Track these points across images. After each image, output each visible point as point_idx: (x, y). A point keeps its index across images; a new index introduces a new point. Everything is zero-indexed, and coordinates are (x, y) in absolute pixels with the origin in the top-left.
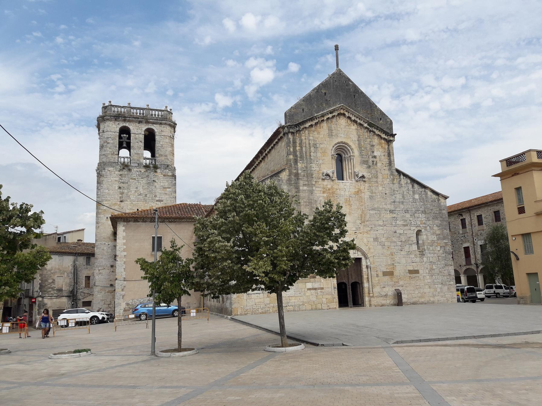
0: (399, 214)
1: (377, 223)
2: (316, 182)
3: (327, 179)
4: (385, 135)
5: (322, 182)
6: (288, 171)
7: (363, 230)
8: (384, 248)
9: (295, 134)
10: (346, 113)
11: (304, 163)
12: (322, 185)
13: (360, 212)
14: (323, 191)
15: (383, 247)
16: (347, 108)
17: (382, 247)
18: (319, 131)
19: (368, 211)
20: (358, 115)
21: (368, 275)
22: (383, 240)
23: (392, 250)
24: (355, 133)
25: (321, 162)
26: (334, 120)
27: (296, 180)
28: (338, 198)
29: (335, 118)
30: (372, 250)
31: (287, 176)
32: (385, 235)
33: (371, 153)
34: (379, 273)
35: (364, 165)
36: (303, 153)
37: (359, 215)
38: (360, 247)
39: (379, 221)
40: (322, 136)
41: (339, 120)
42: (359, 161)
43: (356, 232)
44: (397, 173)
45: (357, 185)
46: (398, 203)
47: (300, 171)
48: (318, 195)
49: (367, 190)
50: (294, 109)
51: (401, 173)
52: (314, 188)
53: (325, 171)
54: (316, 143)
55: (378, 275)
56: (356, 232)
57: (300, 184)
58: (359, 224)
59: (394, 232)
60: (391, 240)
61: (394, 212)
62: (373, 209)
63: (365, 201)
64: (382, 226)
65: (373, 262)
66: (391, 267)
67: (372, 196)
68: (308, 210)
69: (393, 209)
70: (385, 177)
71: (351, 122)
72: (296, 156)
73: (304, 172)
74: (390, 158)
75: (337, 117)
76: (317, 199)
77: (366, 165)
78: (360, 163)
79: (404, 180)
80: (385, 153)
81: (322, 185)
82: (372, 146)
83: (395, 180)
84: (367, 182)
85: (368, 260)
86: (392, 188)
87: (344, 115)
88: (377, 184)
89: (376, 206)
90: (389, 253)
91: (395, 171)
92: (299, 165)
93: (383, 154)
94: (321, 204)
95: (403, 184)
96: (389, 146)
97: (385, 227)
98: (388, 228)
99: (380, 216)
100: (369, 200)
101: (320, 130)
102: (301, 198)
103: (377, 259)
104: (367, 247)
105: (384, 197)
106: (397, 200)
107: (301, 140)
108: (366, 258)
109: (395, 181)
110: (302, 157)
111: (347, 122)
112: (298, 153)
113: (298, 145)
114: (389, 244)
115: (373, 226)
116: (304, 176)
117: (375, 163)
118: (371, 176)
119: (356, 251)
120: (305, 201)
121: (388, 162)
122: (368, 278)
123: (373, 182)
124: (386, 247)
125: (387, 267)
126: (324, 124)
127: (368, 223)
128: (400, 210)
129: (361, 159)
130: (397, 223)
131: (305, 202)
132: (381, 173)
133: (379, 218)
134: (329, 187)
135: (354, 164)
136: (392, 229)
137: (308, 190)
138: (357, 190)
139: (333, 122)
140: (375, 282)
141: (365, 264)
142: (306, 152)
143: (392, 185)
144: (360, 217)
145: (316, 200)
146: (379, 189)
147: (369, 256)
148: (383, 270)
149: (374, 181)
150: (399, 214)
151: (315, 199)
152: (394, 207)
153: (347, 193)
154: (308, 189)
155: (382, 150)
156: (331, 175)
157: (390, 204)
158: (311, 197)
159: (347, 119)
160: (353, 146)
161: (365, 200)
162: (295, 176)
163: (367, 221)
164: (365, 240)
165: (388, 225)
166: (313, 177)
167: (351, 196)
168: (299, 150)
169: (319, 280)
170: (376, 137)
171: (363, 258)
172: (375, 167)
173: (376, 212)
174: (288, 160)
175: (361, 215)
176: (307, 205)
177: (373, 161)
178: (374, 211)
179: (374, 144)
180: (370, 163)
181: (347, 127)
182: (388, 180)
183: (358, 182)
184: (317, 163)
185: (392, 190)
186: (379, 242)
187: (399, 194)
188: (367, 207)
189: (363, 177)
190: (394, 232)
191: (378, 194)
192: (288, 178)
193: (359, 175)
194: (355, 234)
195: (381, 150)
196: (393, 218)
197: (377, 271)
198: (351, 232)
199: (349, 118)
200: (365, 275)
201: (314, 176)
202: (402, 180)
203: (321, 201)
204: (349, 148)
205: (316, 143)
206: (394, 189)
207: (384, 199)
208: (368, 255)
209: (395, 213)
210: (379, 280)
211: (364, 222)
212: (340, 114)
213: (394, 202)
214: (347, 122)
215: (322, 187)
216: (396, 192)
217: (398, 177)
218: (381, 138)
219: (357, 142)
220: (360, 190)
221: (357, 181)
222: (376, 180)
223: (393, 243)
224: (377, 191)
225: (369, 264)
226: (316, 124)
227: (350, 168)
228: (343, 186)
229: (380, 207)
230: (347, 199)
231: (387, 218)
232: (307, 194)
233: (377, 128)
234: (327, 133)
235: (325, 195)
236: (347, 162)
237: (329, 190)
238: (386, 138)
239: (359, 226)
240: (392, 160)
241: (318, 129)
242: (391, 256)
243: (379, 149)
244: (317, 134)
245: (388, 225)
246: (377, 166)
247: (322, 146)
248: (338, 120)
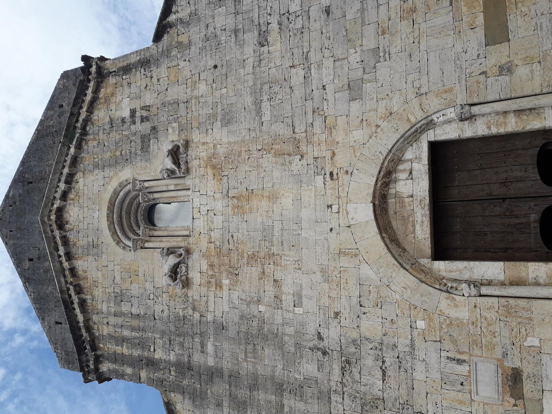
0: (269, 8)
1: (299, 93)
2: (194, 309)
3: (187, 271)
4: (87, 88)
5: (195, 287)
6: (172, 395)
7: (323, 147)
8: (385, 53)
9: (99, 353)
10: (55, 206)
11: (155, 339)
12: (202, 288)
13: (268, 160)
14: (216, 288)
15: (382, 54)
16: (46, 205)
17: (382, 59)
18: (92, 282)
19: (264, 128)
20: (54, 174)
21: (505, 113)
22: (354, 58)
23: (393, 16)
24: (90, 178)
25: (148, 285)
26: (71, 236)
27: (192, 373)
28: (232, 236)
29: (68, 234)
30: (396, 104)
31: (184, 398)
32: (339, 53)
33: (126, 126)
34: (493, 61)
35: (151, 148)
36: (135, 338)
37: (276, 163)
38: (382, 158)
39: (293, 84)
40: (100, 274)
41: (71, 225)
42: (143, 164)
43: (331, 174)
44: (165, 37)
45: (198, 170)
46: (240, 17)
47: (172, 357)
48: (226, 309)
49: (210, 136)
50: (57, 349)
51: (164, 22)
52: (210, 318)
53: (163, 280)
54: (113, 294)
55: (501, 68)
56: (331, 174)
57: (202, 362)
58: (304, 162)
59: (328, 14)
60: (355, 23)
61: (264, 28)
62: (259, 112)
63: (238, 141)
64: (309, 68)
65: (444, 96)
66: (464, 9)
67: (223, 119)
68: (266, 350)
69: (256, 33)
70: (175, 76)
71: (73, 190)
72: (140, 359)
73: (172, 342)
74: (133, 65)
75: (67, 229)
76: (237, 311)
77: (151, 141)
78: (146, 161)
79: (180, 9)
80: (125, 83)
81: (202, 288)
82: (112, 124)
83: (181, 39)
84: (189, 138)
85: (434, 117)
86: (201, 46)
87: (60, 210)
88: (193, 101)
89: (249, 100)
90: (404, 27)
91: (160, 44)
92: (159, 355)
93: (127, 90)
94: (248, 300)
95: (189, 11)
96: (111, 73)
97: (312, 55)
98: (313, 44)
99: (276, 82)
100: (233, 127)
101: (90, 279)
102: (236, 368)
103: (431, 79)
104: (384, 124)
105: (224, 71)
106: (230, 22)
107: (111, 336)
108: (430, 125)
109: (183, 39)
110: (142, 344)
111: (73, 200)
112: (137, 353)
113: (119, 349)
114: (370, 31)
115: (309, 103)
116: (182, 345)
117: (145, 113)
118: (175, 125)
119: (401, 167)
120: (243, 357)
121: (142, 70)
122: (519, 112)
123: (189, 116)
124: (383, 42)
125: (465, 26)
126: (80, 264)
127: (300, 128)
128: (259, 7)
129: (139, 158)
130: (299, 8)
131: (246, 355)
132: (167, 90)
133: (284, 83)
134: (205, 267)
135: (152, 179)
136: (317, 25)
137: (216, 339)
138: (209, 170)
139: (75, 240)
140: (537, 81)
141: (454, 125)
142: (133, 329)
143: (193, 48)
144: (280, 160)
145: (242, 317)
146: (204, 94)
147: (420, 115)
148: (479, 45)
149: (184, 114)
150: (269, 8)
151: (236, 320)
152: (249, 31)
153: (219, 205)
154: (212, 340)
155: (118, 93)
156: (172, 260)
157: (242, 46)
158: (232, 332)
159: (68, 202)
160: (114, 184)
161: (235, 143)
162: (183, 374)
163: (294, 132)
164: (358, 135)
165: (306, 44)
166: (184, 317)
167: (225, 192)
168: (128, 348)
169: (529, 358)
170: (95, 117)
171: (432, 136)
172: (154, 110)
173: (265, 98)
174: (151, 382)
175: (278, 154)
176: (254, 351)
177: (144, 119)
178: (263, 104)
179: (107, 119)
180: (147, 126)
181: (81, 201)
182: (182, 64)
183: (190, 166)
184: (152, 296)
185: (205, 47)
186: (366, 77)
187: (213, 17)
188: (253, 134)
189: (174, 154)
190: (328, 14)
191: (217, 94)
192: (190, 398)
193: (169, 167)
194: (335, 176)
195: (119, 98)
196: (283, 27)
197: (484, 73)
198: (329, 192)
199: (64, 196)
200: (505, 124)
201: (181, 314)
202: (180, 15)
203: (242, 299)
204: (122, 194)
205: (113, 294)
206: (203, 41)
207: (230, 72)
208: (413, 120)
209: (268, 24)
210: (529, 61)
211: (297, 143)
212: (58, 222)
213: (236, 31)
214: (73, 200)
215: (206, 289)
216: (211, 29)
217: (173, 31)
218: (94, 100)
219: (107, 172)
220: (210, 158)
221: (188, 171)
222: (182, 105)
223: (366, 12)
224: (210, 100)
225: (451, 113)
226: (79, 290)
227: (165, 188)
228: (202, 219)
229: (251, 83)
230: (234, 207)
231: (284, 52)
232: (226, 346)
233: (74, 115)
234: (94, 259)
235: (226, 282)
236: (156, 196)
237: (211, 266)
238: (92, 84)
239: (311, 161)
240: (138, 58)
241: (89, 283)
242: (419, 17)
243: (117, 103)
244: (97, 289)
245: (306, 44)
246: (152, 106)
247: (118, 280)
248: (72, 227)
